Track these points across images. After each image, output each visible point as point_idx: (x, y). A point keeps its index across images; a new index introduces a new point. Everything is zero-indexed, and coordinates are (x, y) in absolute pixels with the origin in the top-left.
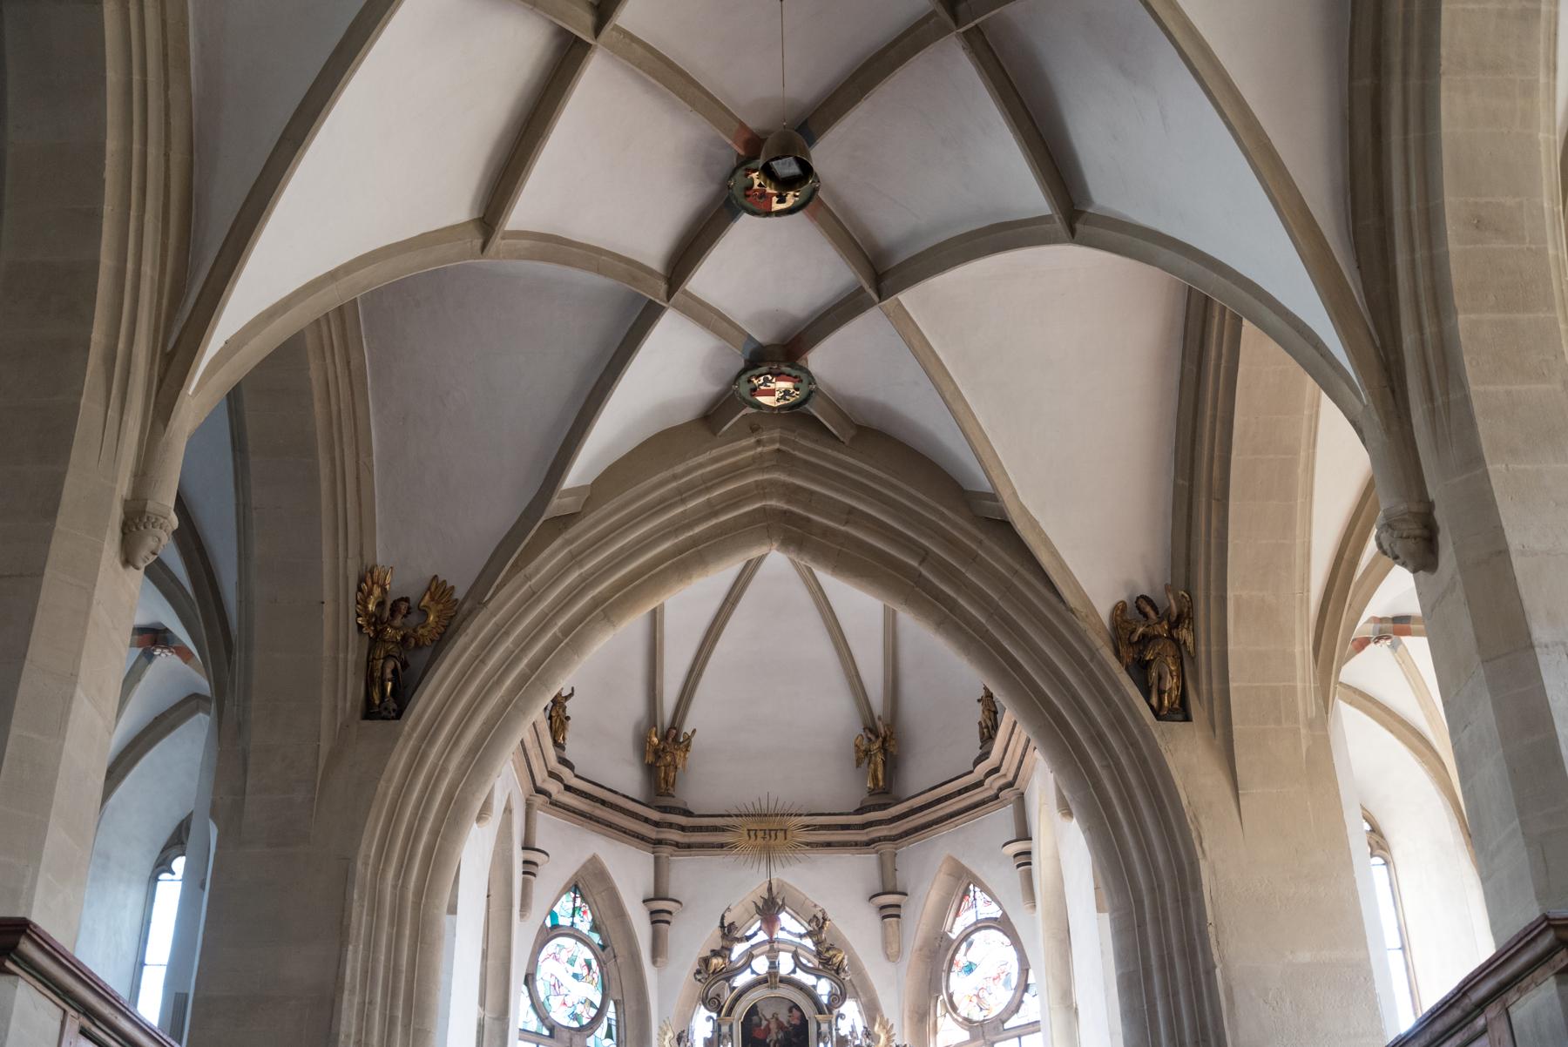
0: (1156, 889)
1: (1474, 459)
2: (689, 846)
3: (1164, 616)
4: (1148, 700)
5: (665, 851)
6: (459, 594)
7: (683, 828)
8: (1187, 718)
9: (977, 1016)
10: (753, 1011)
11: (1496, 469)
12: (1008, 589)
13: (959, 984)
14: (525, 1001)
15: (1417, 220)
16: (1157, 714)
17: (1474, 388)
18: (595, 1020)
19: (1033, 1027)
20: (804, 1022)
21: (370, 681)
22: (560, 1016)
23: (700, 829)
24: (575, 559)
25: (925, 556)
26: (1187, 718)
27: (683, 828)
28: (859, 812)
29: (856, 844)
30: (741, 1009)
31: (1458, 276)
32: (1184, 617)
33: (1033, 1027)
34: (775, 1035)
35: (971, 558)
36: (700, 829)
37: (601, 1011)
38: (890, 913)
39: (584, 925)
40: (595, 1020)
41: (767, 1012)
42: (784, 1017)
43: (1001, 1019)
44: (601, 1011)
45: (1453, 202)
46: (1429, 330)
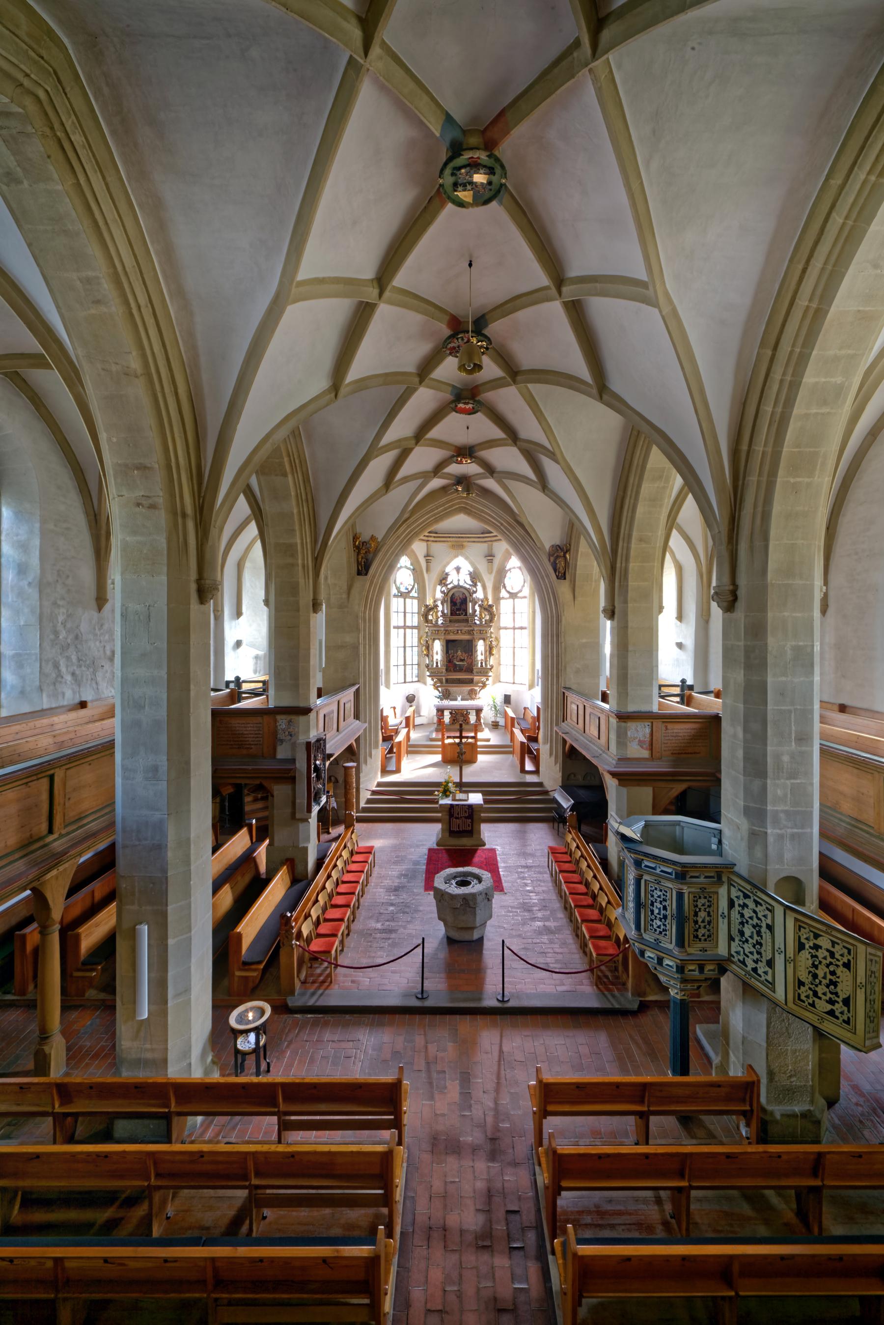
0: (552, 617)
1: (626, 602)
2: (436, 541)
3: (562, 550)
4: (555, 572)
5: (429, 543)
6: (379, 540)
7: (434, 537)
8: (565, 579)
9: (511, 591)
10: (453, 594)
11: (630, 605)
12: (523, 538)
13: (507, 581)
14: (394, 587)
15: (626, 535)
16: (558, 577)
17: (630, 583)
18: (412, 589)
19: (525, 597)
20: (466, 598)
21: (358, 563)
22: (403, 590)
23: (439, 537)
24: (408, 527)
25: (502, 524)
26: (565, 579)
27: (434, 537)
28: (482, 533)
29: (482, 542)
30: (450, 594)
31: (633, 553)
32: (568, 550)
33: (525, 597)
34: (458, 601)
35: (514, 528)
36: (439, 537)
37: (413, 587)
38: (490, 561)
39: (409, 565)
40: (412, 589)
41: (457, 595)
42: (461, 596)
43: (517, 593)
44: (413, 587)
45: (635, 534)
46: (624, 565)
